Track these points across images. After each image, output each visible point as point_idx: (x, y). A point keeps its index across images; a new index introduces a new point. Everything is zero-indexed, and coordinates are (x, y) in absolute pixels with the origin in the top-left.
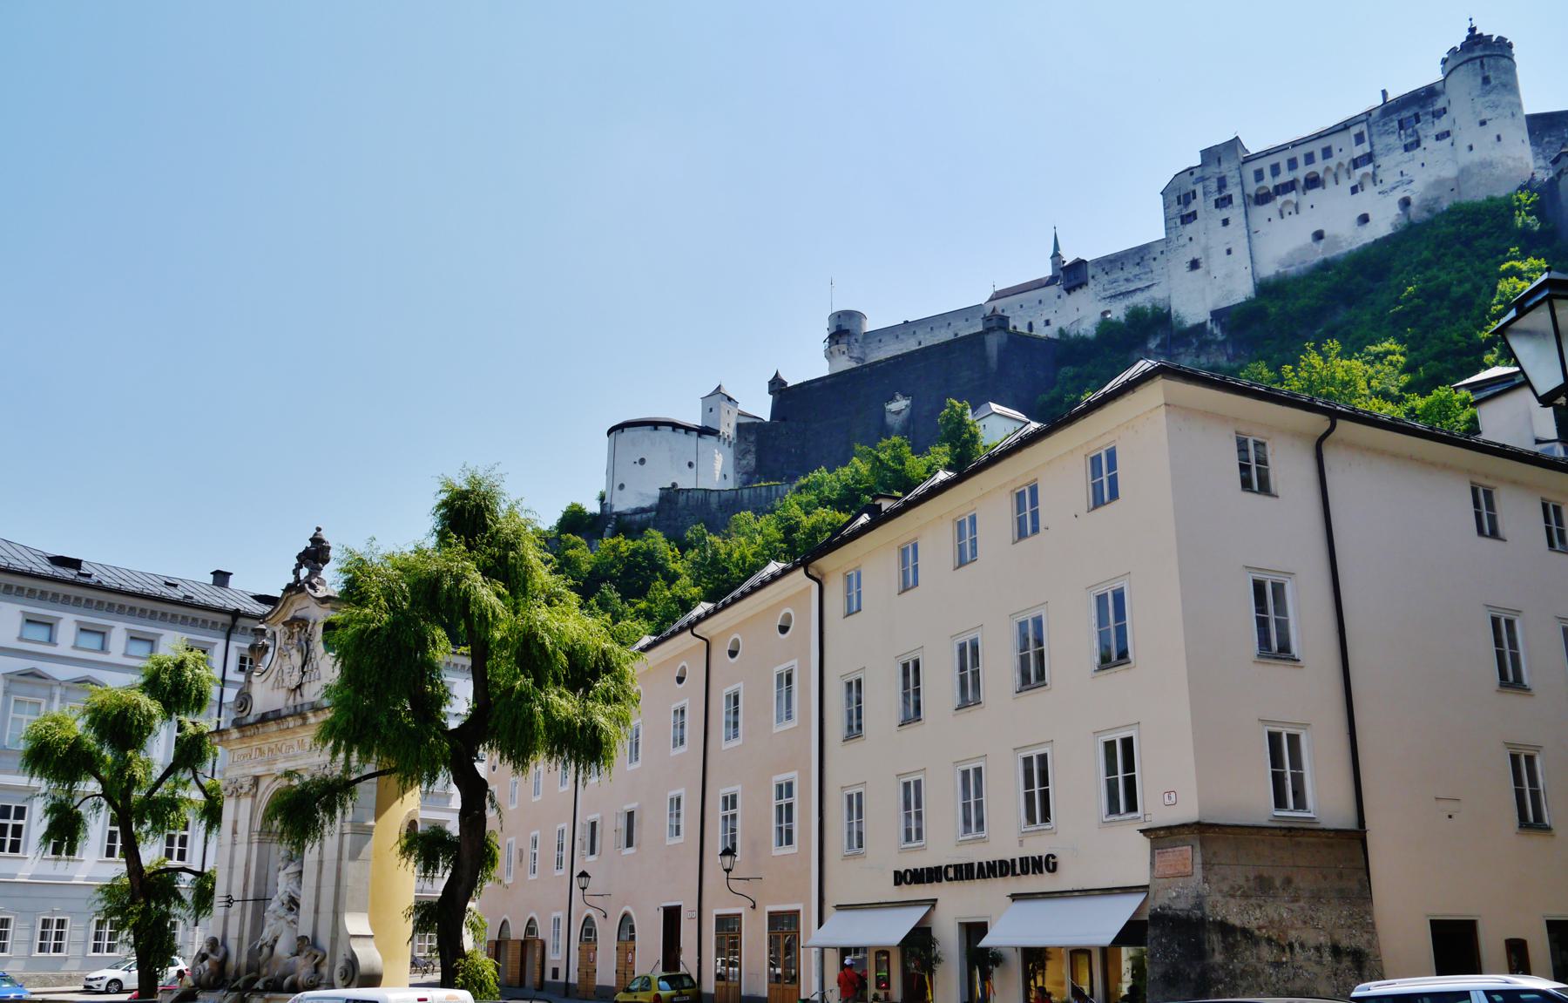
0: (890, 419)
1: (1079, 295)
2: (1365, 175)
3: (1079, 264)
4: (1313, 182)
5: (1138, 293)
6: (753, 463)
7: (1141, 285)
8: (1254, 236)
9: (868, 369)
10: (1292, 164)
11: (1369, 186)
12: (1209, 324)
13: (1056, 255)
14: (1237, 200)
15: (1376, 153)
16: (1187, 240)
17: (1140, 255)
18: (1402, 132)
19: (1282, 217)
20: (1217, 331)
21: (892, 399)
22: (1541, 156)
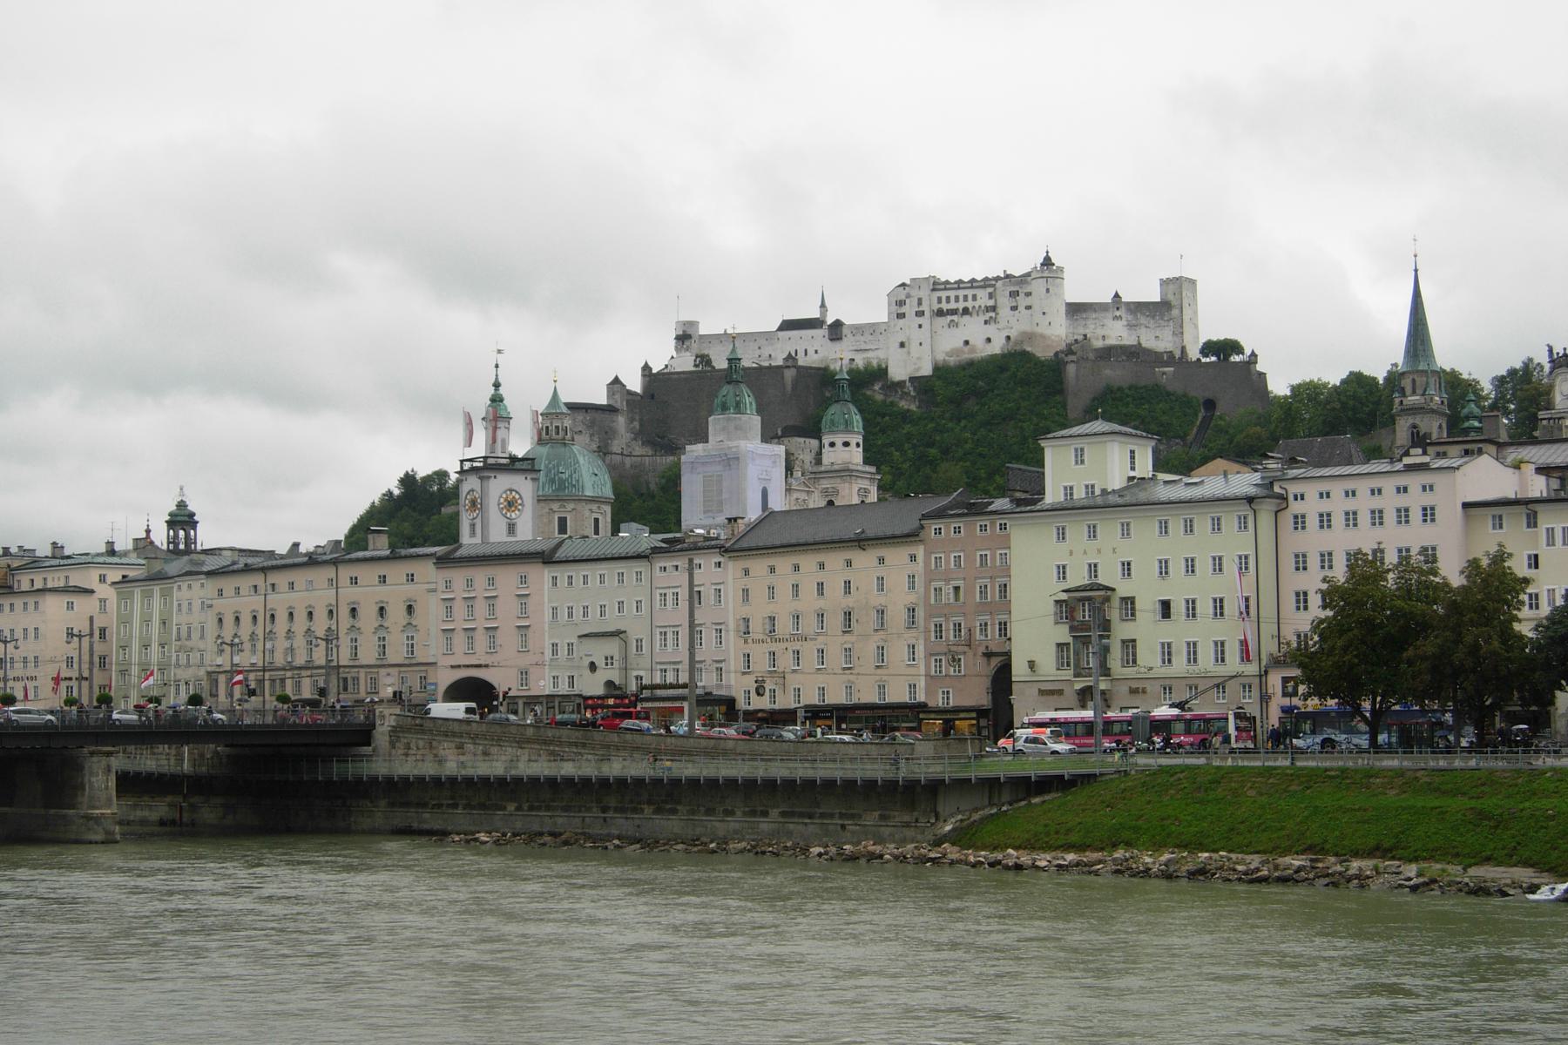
1: (837, 346)
2: (991, 317)
3: (838, 324)
4: (966, 311)
6: (638, 427)
7: (873, 347)
12: (908, 384)
13: (823, 305)
14: (927, 314)
17: (873, 329)
20: (911, 389)
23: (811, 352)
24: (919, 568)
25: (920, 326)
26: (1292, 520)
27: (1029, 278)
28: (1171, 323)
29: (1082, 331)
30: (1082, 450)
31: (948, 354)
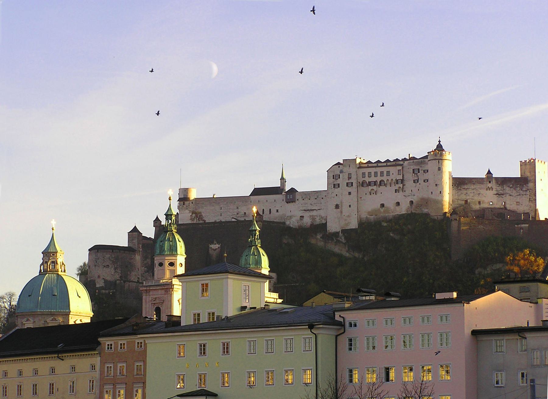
0: (211, 252)
1: (291, 205)
3: (293, 191)
4: (381, 183)
5: (315, 211)
8: (359, 199)
9: (201, 226)
10: (376, 174)
11: (401, 192)
12: (340, 233)
13: (282, 179)
14: (355, 185)
15: (404, 179)
16: (335, 195)
17: (316, 194)
18: (413, 174)
19: (371, 195)
20: (343, 238)
21: (212, 243)
22: (457, 194)
23: (274, 211)
24: (96, 374)
25: (350, 193)
26: (347, 343)
27: (427, 160)
28: (528, 193)
29: (464, 197)
30: (207, 285)
31: (370, 213)
